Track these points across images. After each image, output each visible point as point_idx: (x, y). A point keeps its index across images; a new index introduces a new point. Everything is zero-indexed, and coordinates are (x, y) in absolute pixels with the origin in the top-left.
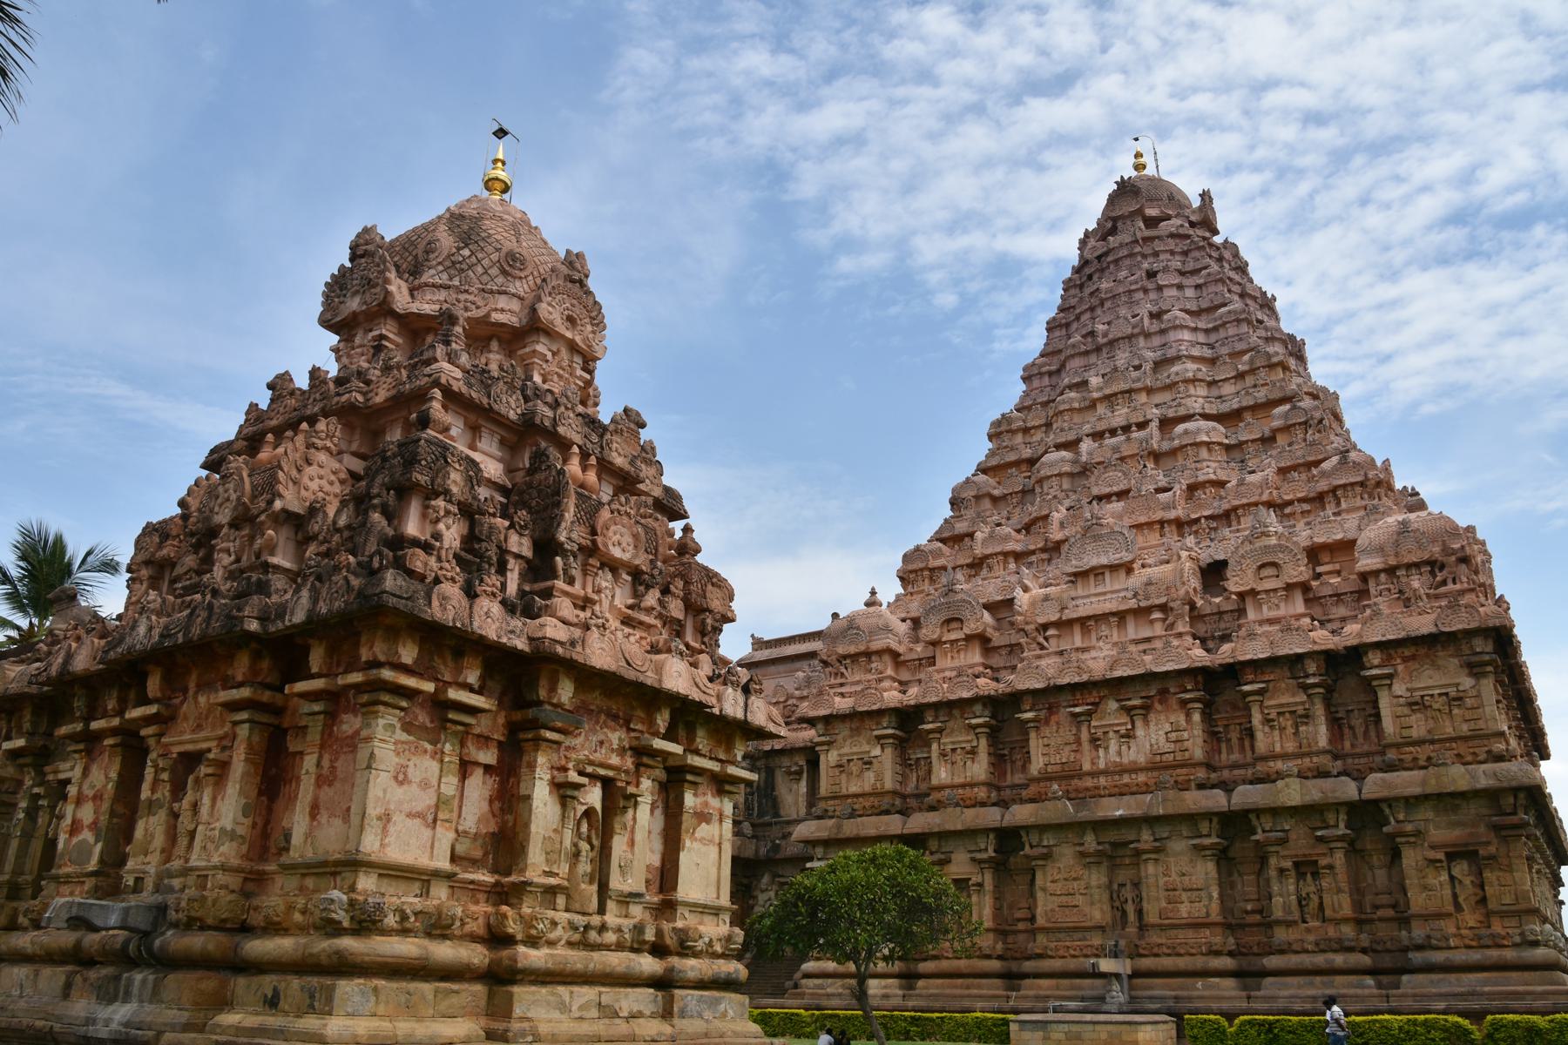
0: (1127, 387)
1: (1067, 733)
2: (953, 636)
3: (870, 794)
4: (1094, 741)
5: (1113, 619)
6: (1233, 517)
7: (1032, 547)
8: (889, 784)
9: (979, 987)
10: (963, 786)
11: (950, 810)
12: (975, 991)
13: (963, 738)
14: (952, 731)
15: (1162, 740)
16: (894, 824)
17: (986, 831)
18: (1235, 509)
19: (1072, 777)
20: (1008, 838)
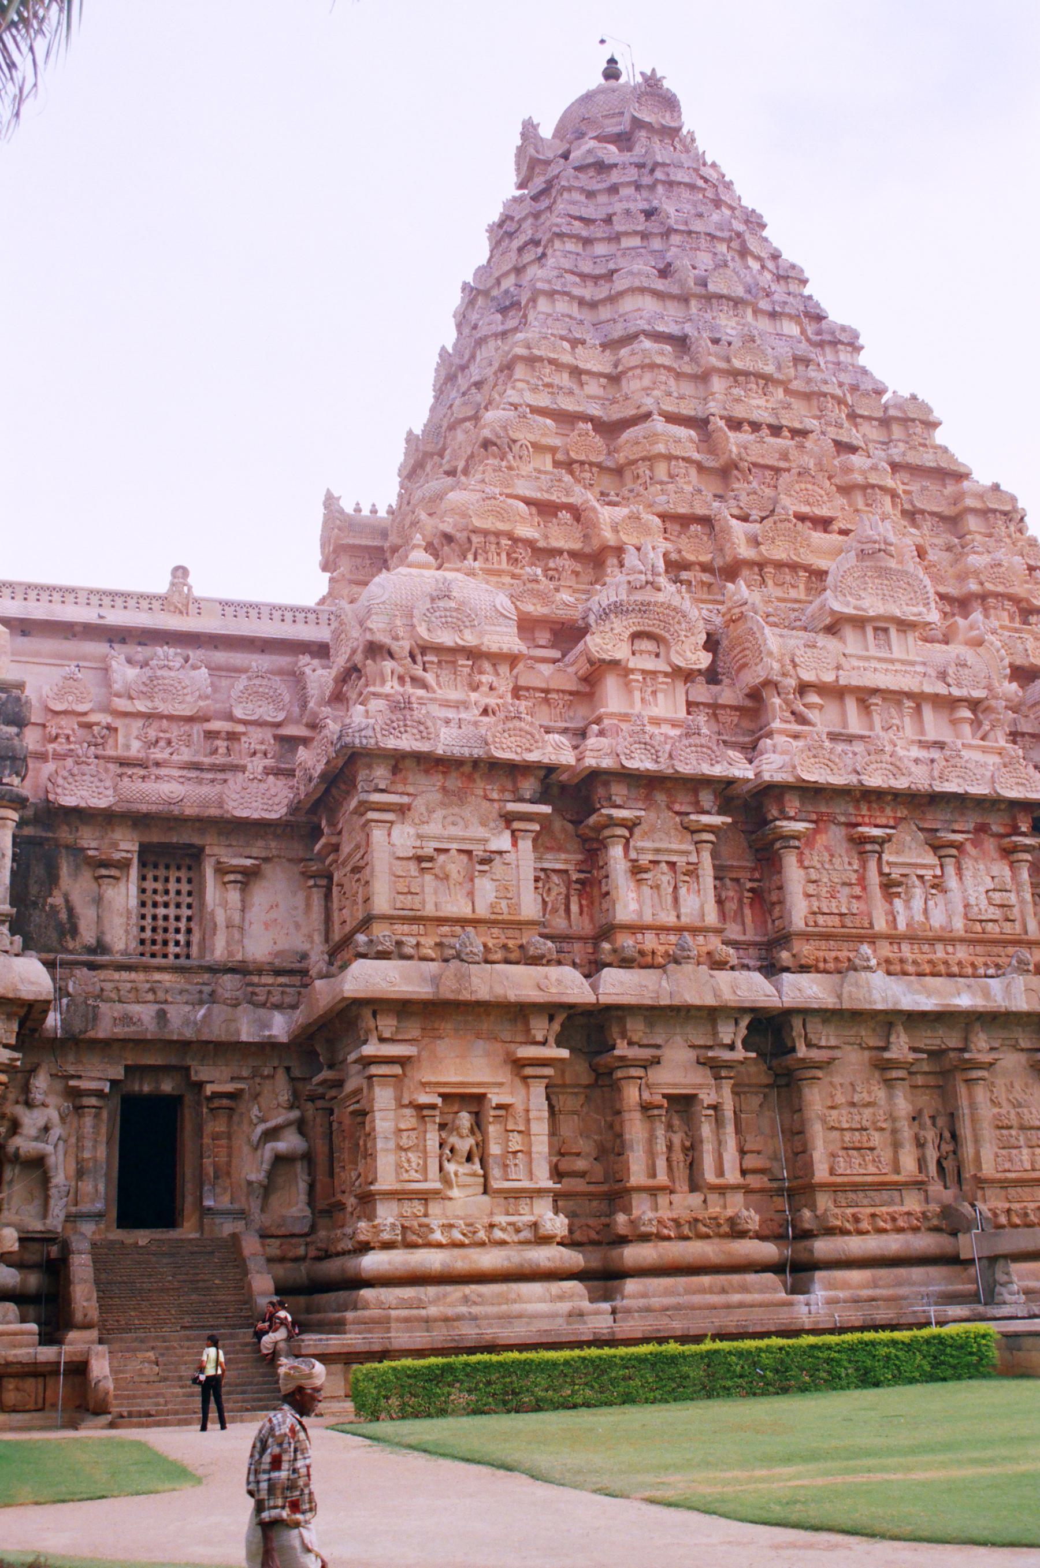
0: (770, 369)
1: (845, 865)
2: (650, 664)
3: (494, 923)
4: (890, 887)
5: (909, 703)
6: (976, 605)
7: (691, 558)
8: (530, 907)
9: (744, 1289)
10: (679, 930)
11: (688, 968)
12: (736, 1298)
13: (678, 845)
14: (653, 829)
15: (984, 902)
16: (567, 984)
17: (735, 1013)
18: (983, 597)
19: (861, 939)
20: (770, 1029)
